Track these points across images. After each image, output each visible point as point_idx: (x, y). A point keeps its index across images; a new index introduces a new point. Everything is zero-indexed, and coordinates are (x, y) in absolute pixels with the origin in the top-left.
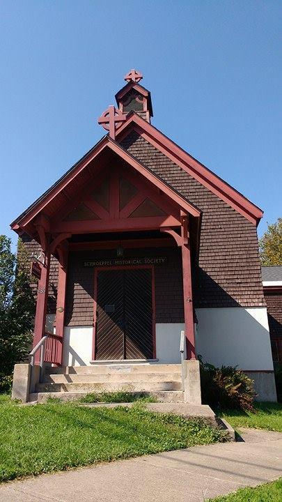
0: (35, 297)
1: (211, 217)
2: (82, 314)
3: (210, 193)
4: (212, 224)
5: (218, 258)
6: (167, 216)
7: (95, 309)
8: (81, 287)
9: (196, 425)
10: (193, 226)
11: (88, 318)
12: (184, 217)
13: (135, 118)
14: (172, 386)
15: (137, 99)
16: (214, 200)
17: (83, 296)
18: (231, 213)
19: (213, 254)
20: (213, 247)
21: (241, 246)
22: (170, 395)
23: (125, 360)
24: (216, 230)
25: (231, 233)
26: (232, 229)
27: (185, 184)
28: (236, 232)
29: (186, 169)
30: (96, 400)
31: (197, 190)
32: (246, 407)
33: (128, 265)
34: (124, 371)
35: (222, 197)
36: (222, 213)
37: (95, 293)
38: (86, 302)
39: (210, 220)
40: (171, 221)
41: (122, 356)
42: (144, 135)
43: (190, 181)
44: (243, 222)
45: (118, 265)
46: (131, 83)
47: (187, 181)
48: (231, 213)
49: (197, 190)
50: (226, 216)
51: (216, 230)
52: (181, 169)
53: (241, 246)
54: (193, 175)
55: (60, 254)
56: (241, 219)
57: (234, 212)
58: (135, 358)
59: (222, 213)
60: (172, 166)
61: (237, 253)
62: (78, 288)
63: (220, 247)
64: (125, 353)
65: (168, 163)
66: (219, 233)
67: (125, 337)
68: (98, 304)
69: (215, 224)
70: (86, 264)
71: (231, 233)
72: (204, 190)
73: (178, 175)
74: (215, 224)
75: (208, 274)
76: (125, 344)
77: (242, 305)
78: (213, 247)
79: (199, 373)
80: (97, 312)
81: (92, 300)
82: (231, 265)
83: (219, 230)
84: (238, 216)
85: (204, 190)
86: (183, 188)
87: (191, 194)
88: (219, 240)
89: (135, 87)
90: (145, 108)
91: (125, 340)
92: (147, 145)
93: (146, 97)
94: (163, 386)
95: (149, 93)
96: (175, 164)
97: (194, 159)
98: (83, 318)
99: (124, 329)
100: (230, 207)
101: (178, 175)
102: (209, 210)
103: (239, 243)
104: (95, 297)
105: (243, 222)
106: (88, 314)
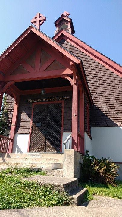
0: (10, 122)
1: (102, 78)
2: (24, 127)
3: (102, 66)
4: (102, 82)
5: (105, 100)
6: (66, 69)
7: (31, 125)
8: (25, 113)
9: (47, 191)
10: (79, 69)
11: (27, 130)
12: (72, 66)
13: (63, 32)
14: (59, 166)
15: (65, 24)
16: (104, 69)
17: (26, 118)
18: (114, 75)
19: (103, 98)
20: (103, 94)
21: (119, 93)
22: (55, 171)
23: (45, 153)
24: (104, 85)
25: (113, 86)
26: (114, 84)
27: (88, 62)
28: (116, 86)
29: (89, 54)
30: (10, 172)
31: (95, 65)
32: (109, 182)
33: (50, 101)
34: (37, 157)
35: (108, 67)
36: (108, 76)
37: (32, 116)
38: (27, 121)
39: (101, 80)
40: (68, 71)
41: (44, 151)
42: (68, 40)
43: (91, 60)
44: (120, 80)
45: (45, 101)
46: (63, 16)
47: (89, 61)
48: (114, 75)
49: (95, 65)
50: (110, 77)
51: (104, 85)
52: (86, 55)
53: (119, 93)
54: (93, 57)
55: (14, 95)
56: (119, 78)
57: (115, 75)
58: (50, 152)
59: (108, 76)
60: (82, 54)
61: (116, 97)
62: (24, 114)
63: (107, 94)
64: (45, 149)
65: (80, 52)
66: (106, 87)
67: (46, 140)
68: (33, 122)
69: (104, 82)
70: (28, 101)
71: (113, 86)
72: (99, 64)
73: (85, 58)
74: (104, 82)
75: (99, 108)
76: (46, 144)
77: (119, 125)
78: (103, 94)
79: (73, 157)
80: (32, 127)
81: (30, 120)
82: (112, 103)
83: (106, 85)
84: (117, 77)
85: (99, 64)
86: (87, 64)
87: (92, 67)
88: (106, 90)
89: (65, 18)
90: (69, 27)
91: (46, 142)
92: (69, 45)
93: (70, 22)
94: (54, 166)
95: (71, 20)
96: (83, 53)
97: (93, 49)
98: (25, 130)
99: (45, 136)
100: (113, 72)
101: (85, 58)
102: (101, 75)
103: (118, 91)
104: (32, 118)
105: (120, 80)
106: (28, 127)
